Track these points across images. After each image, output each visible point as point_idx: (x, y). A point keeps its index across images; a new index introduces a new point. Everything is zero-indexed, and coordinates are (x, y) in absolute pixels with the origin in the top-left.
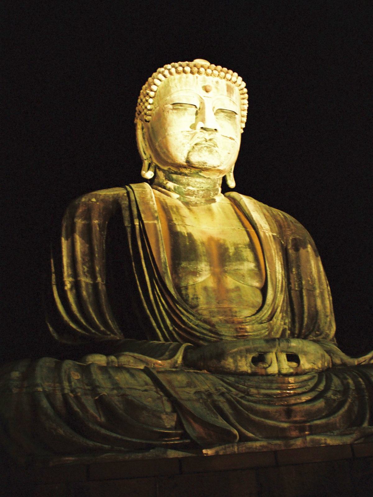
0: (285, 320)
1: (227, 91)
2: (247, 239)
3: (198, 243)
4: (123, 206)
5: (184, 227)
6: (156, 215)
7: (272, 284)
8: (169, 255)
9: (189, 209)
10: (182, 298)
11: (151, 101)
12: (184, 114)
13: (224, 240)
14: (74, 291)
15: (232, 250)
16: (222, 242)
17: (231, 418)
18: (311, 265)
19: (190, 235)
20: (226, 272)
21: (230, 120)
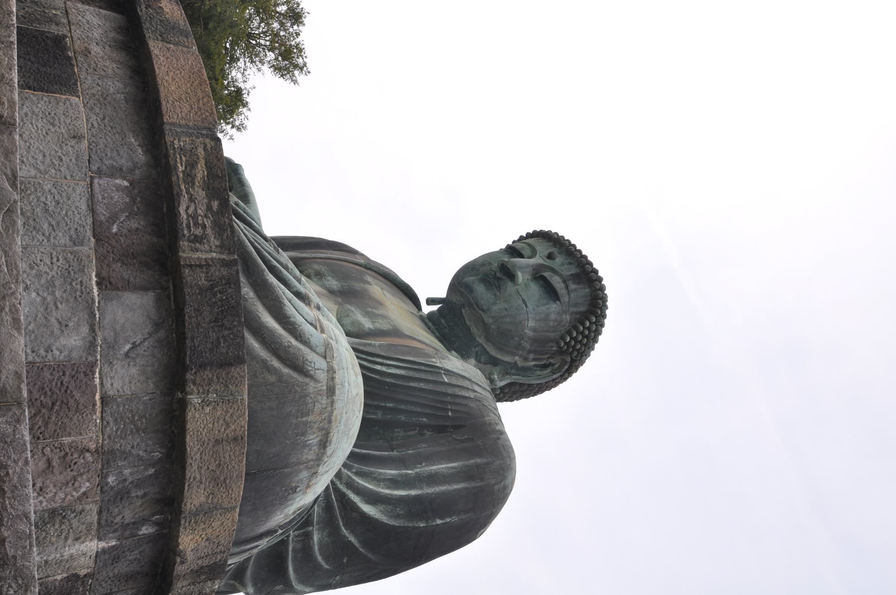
1: (571, 275)
2: (407, 333)
7: (360, 344)
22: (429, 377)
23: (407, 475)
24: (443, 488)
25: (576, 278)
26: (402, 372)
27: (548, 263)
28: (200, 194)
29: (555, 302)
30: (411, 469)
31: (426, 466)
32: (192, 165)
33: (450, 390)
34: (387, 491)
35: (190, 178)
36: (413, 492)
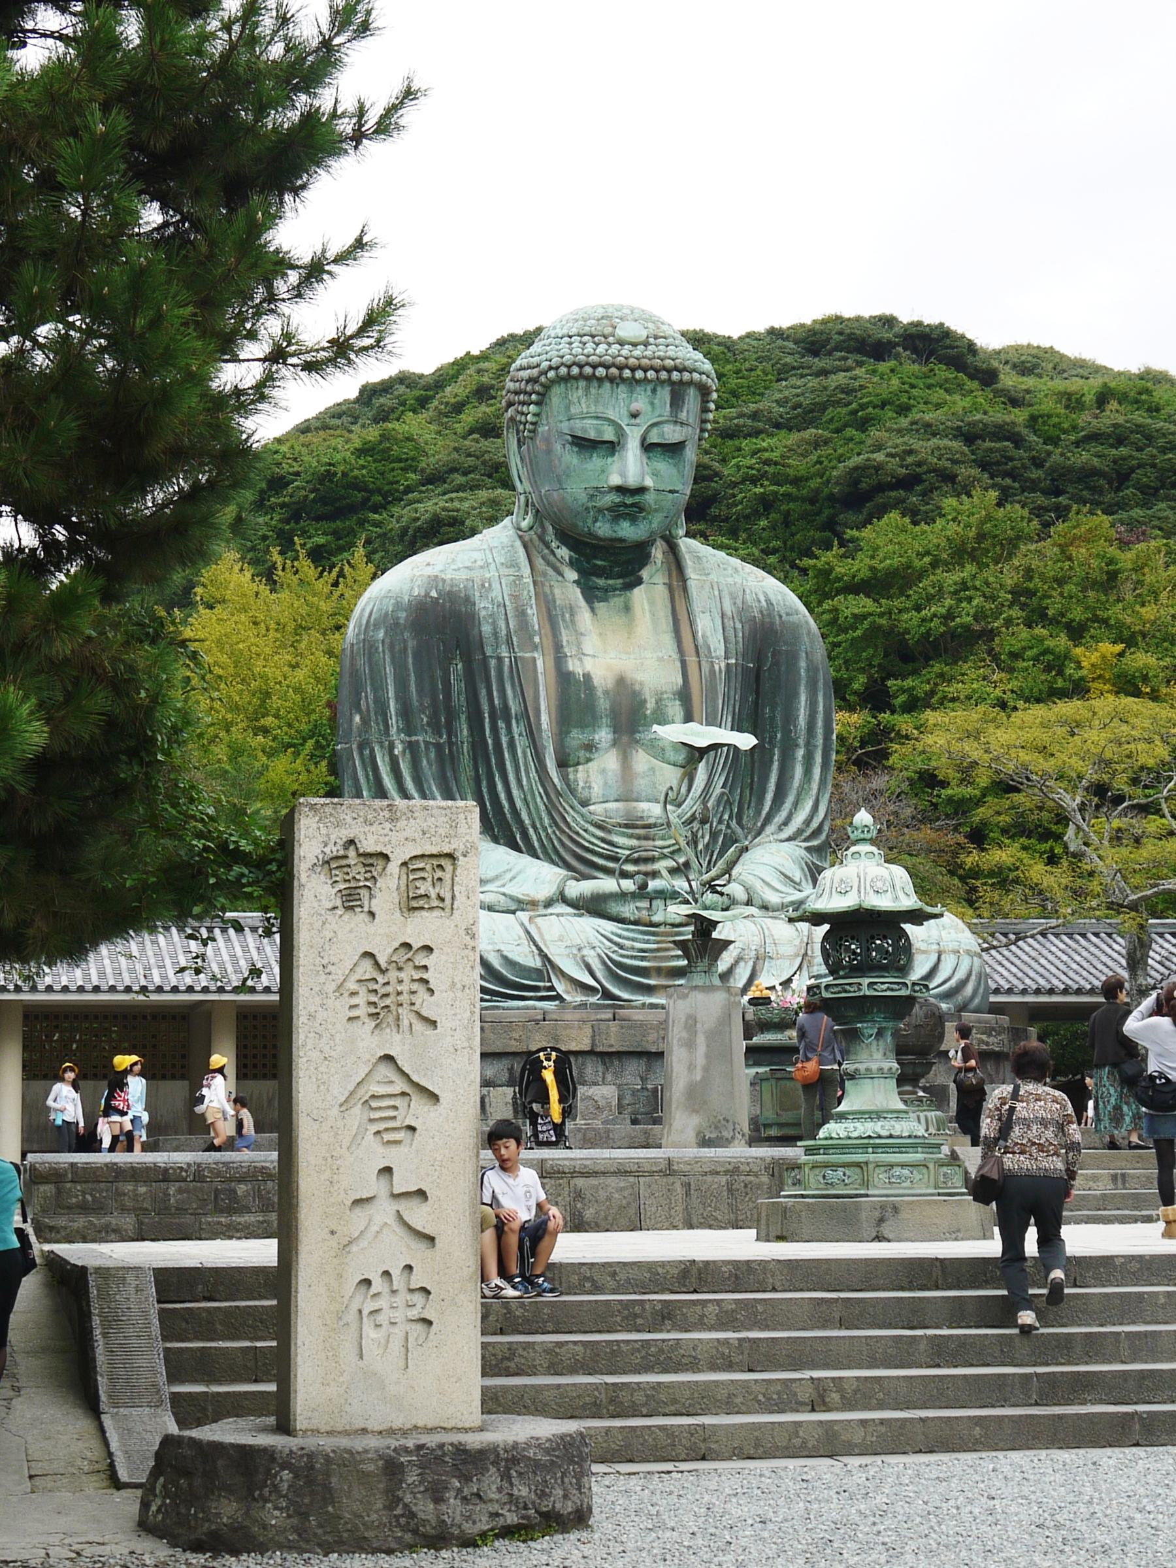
0: (723, 813)
2: (680, 681)
3: (600, 693)
4: (483, 613)
5: (581, 660)
6: (537, 639)
8: (553, 716)
9: (592, 609)
10: (568, 785)
11: (532, 408)
12: (591, 457)
13: (641, 684)
14: (408, 756)
15: (650, 705)
16: (637, 687)
17: (599, 975)
18: (799, 703)
19: (587, 677)
20: (637, 742)
21: (672, 458)
22: (732, 685)
23: (803, 757)
24: (820, 723)
25: (677, 401)
26: (730, 719)
27: (644, 422)
28: (991, 1040)
29: (684, 447)
30: (797, 746)
31: (795, 727)
32: (983, 1042)
33: (740, 662)
34: (815, 786)
35: (987, 1044)
36: (818, 759)
